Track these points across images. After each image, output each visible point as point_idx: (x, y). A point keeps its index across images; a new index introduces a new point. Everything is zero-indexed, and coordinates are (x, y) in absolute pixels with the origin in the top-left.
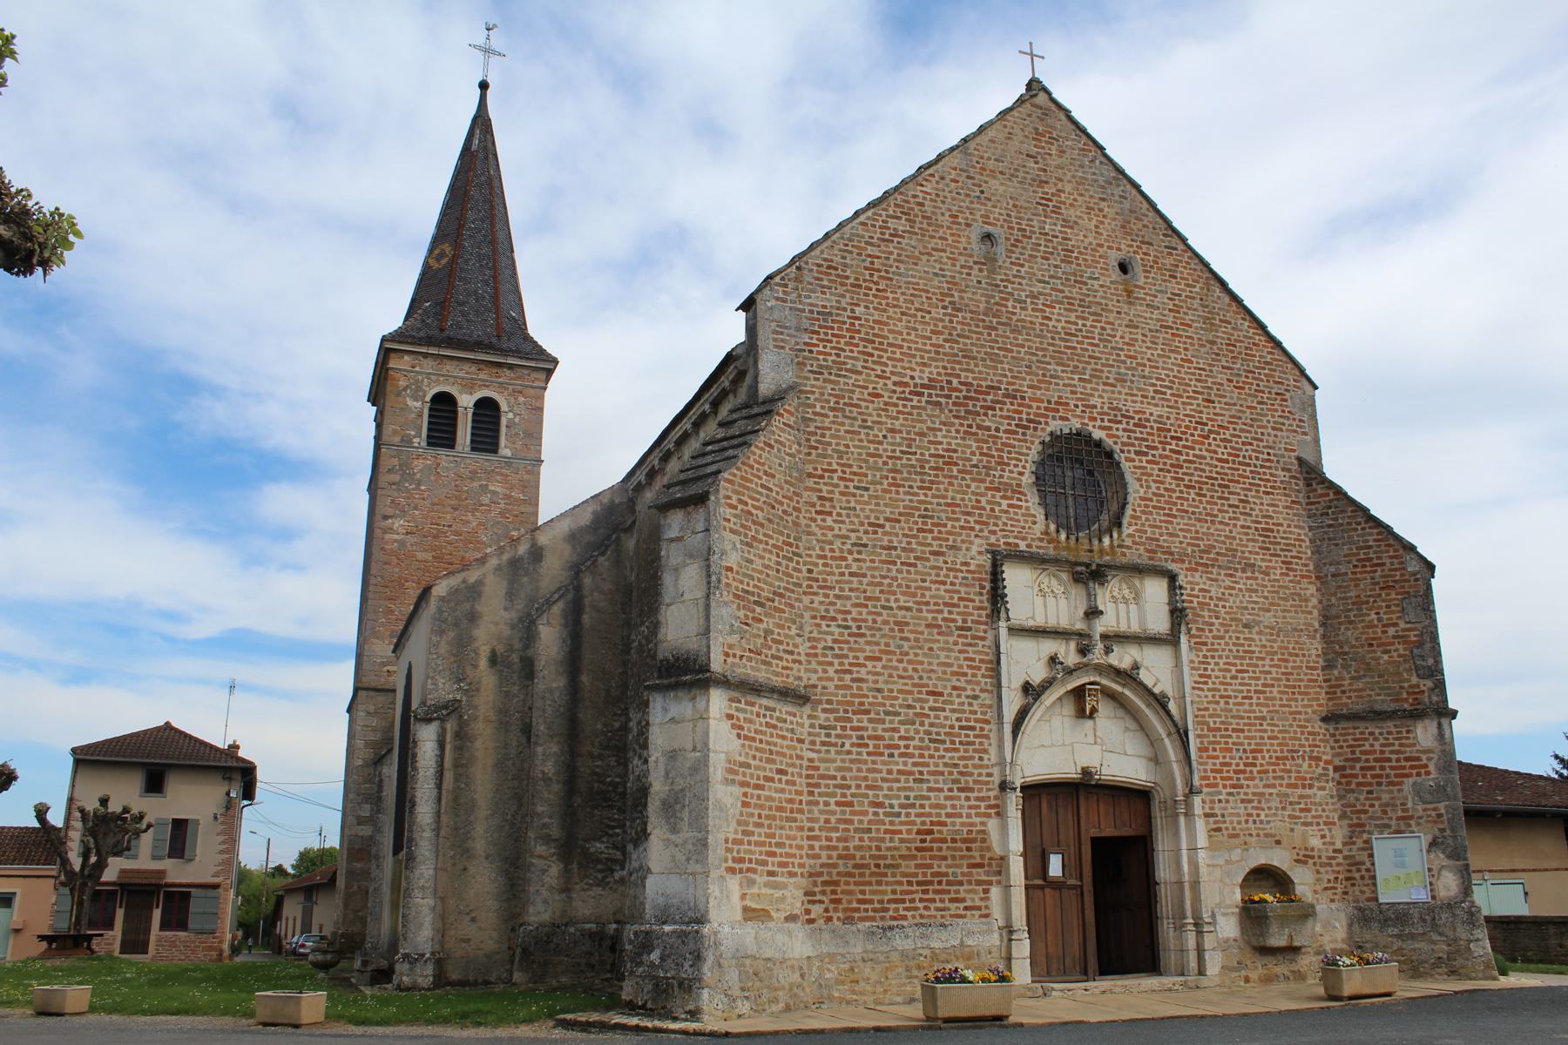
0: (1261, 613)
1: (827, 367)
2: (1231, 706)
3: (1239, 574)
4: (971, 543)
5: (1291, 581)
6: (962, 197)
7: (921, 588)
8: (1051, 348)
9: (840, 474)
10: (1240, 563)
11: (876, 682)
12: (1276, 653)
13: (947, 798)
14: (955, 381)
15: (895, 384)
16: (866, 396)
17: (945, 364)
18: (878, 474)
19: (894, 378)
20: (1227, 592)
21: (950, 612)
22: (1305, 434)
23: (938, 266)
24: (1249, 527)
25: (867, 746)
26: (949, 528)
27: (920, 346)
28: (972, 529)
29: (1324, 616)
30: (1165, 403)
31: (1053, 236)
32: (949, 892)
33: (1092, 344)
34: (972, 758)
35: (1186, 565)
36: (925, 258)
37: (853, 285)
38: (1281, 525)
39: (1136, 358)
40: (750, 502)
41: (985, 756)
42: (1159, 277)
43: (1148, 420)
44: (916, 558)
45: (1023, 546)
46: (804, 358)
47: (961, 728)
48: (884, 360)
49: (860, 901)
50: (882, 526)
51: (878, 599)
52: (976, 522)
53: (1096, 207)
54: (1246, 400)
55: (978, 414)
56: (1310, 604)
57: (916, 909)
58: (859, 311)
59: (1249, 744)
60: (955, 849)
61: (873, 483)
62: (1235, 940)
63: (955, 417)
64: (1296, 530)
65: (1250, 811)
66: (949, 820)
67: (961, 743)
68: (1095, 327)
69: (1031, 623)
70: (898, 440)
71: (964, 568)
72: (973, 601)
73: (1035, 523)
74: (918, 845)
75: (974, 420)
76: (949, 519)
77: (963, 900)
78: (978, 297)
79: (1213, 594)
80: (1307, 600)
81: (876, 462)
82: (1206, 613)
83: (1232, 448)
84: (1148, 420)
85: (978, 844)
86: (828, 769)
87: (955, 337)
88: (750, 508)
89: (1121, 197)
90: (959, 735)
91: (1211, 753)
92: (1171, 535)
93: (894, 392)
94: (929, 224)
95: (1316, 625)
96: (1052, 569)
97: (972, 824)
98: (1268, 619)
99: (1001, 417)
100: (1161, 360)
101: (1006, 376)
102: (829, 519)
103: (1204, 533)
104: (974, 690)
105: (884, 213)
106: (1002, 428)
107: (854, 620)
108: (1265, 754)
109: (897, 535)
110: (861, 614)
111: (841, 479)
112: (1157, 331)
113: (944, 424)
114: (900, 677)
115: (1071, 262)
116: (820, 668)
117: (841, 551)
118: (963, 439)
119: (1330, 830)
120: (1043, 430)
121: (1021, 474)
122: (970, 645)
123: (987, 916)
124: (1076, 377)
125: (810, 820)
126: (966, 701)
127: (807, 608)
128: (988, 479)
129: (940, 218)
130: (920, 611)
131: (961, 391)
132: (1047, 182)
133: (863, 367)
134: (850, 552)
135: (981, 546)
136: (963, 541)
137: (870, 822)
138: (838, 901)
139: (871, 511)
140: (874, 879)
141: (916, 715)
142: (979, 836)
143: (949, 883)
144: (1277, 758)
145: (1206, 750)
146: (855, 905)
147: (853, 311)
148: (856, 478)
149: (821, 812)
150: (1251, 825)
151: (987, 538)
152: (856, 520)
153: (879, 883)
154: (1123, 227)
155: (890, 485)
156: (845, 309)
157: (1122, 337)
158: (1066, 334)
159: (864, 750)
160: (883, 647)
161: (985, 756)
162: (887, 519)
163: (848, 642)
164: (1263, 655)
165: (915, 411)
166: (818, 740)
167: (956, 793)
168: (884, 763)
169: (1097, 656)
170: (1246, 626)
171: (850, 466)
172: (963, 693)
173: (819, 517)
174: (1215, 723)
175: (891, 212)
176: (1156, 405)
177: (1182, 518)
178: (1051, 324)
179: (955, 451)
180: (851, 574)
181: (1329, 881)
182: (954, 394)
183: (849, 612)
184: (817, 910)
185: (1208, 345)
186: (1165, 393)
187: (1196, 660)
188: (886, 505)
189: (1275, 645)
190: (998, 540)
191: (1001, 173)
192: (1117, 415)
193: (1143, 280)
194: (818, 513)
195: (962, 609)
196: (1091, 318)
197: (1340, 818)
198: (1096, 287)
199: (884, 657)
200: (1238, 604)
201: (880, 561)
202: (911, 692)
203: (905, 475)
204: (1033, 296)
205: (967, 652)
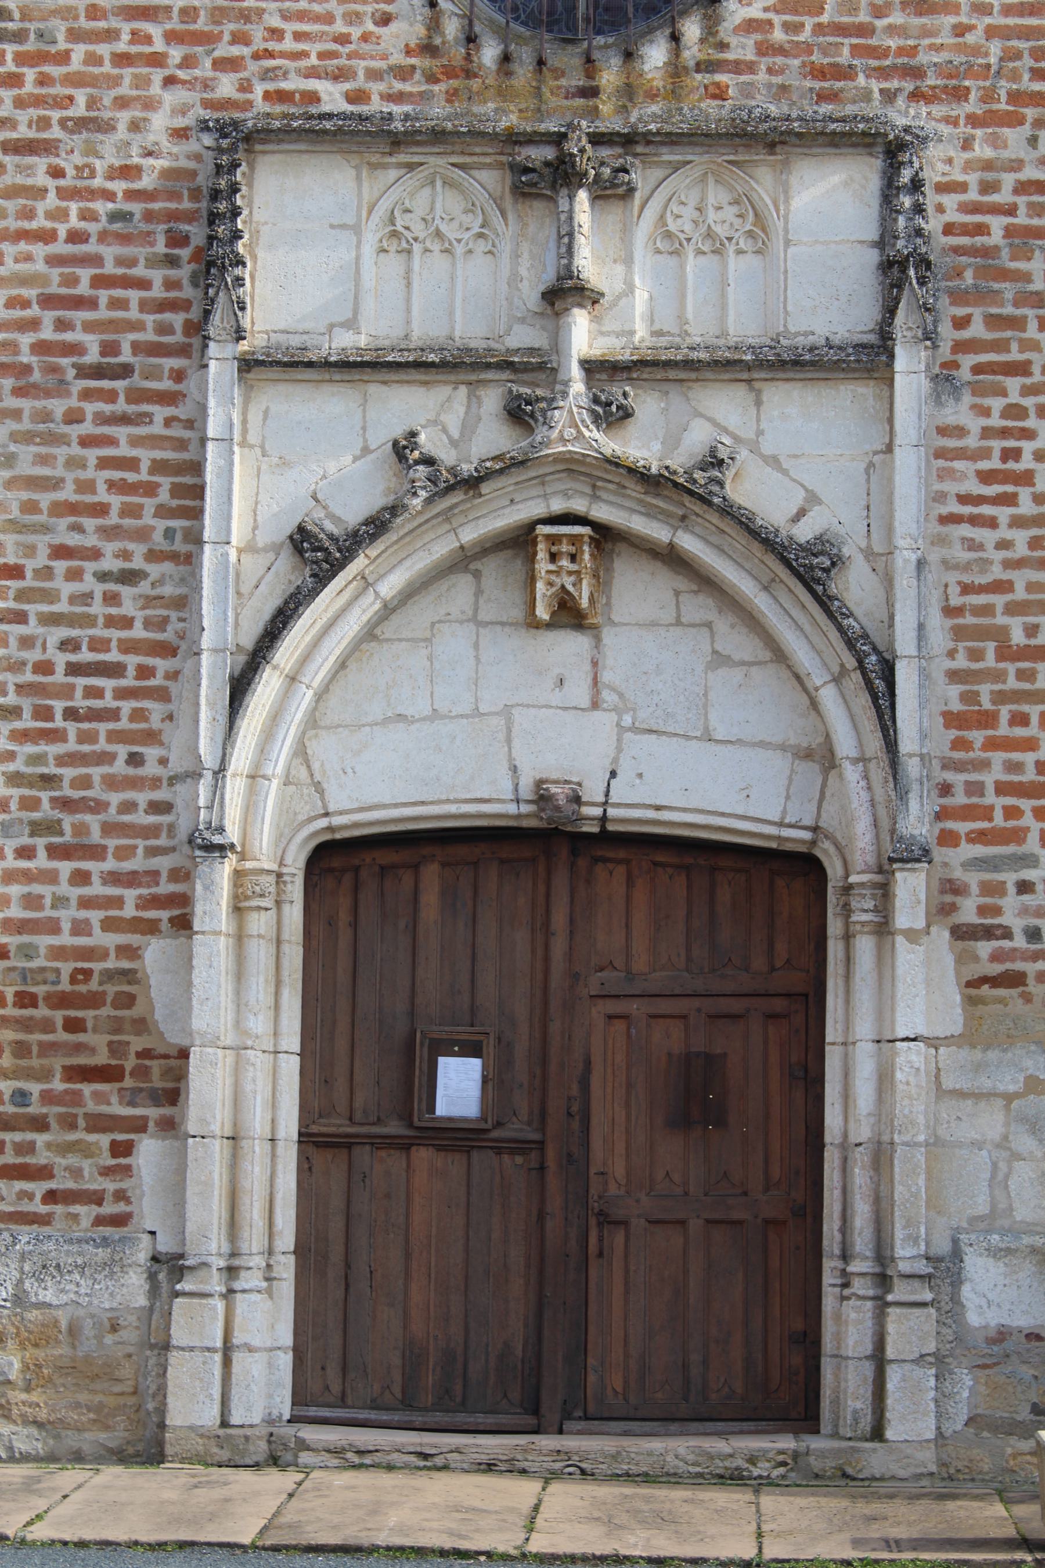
4: (150, 105)
21: (62, 325)
28: (157, 60)
35: (972, 106)
47: (74, 669)
52: (171, 37)
67: (71, 714)
71: (119, 186)
72: (143, 284)
73: (385, 20)
76: (75, 35)
77: (44, 1173)
85: (106, 1011)
90: (67, 691)
91: (1003, 729)
96: (437, 162)
104: (126, 555)
122: (124, 419)
123: (120, 1220)
126: (99, 589)
142: (111, 989)
145: (988, 719)
151: (206, 85)
161: (151, 753)
172: (90, 567)
187: (975, 424)
190: (245, 87)
195: (103, 313)
205: (112, 442)
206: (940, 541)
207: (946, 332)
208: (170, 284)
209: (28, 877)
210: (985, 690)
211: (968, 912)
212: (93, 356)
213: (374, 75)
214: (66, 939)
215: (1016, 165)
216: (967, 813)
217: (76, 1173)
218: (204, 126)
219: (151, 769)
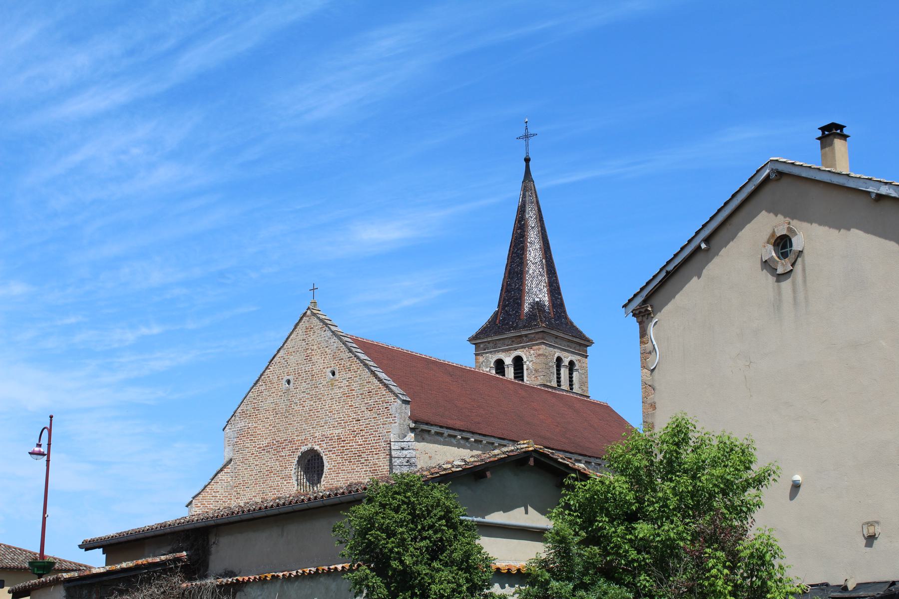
9: (242, 484)
16: (250, 455)
19: (258, 446)
22: (395, 423)
23: (272, 399)
24: (367, 471)
33: (318, 412)
38: (380, 466)
39: (332, 412)
40: (206, 503)
43: (334, 436)
55: (280, 452)
76: (269, 492)
83: (365, 438)
84: (334, 436)
88: (206, 505)
92: (338, 481)
93: (258, 451)
99: (287, 451)
101: (289, 434)
102: (239, 500)
111: (243, 486)
113: (270, 458)
118: (275, 462)
120: (299, 451)
121: (291, 470)
132: (308, 349)
133: (250, 445)
158: (310, 410)
176: (337, 429)
177: (342, 473)
179: (273, 467)
185: (360, 396)
186: (341, 423)
196: (318, 401)
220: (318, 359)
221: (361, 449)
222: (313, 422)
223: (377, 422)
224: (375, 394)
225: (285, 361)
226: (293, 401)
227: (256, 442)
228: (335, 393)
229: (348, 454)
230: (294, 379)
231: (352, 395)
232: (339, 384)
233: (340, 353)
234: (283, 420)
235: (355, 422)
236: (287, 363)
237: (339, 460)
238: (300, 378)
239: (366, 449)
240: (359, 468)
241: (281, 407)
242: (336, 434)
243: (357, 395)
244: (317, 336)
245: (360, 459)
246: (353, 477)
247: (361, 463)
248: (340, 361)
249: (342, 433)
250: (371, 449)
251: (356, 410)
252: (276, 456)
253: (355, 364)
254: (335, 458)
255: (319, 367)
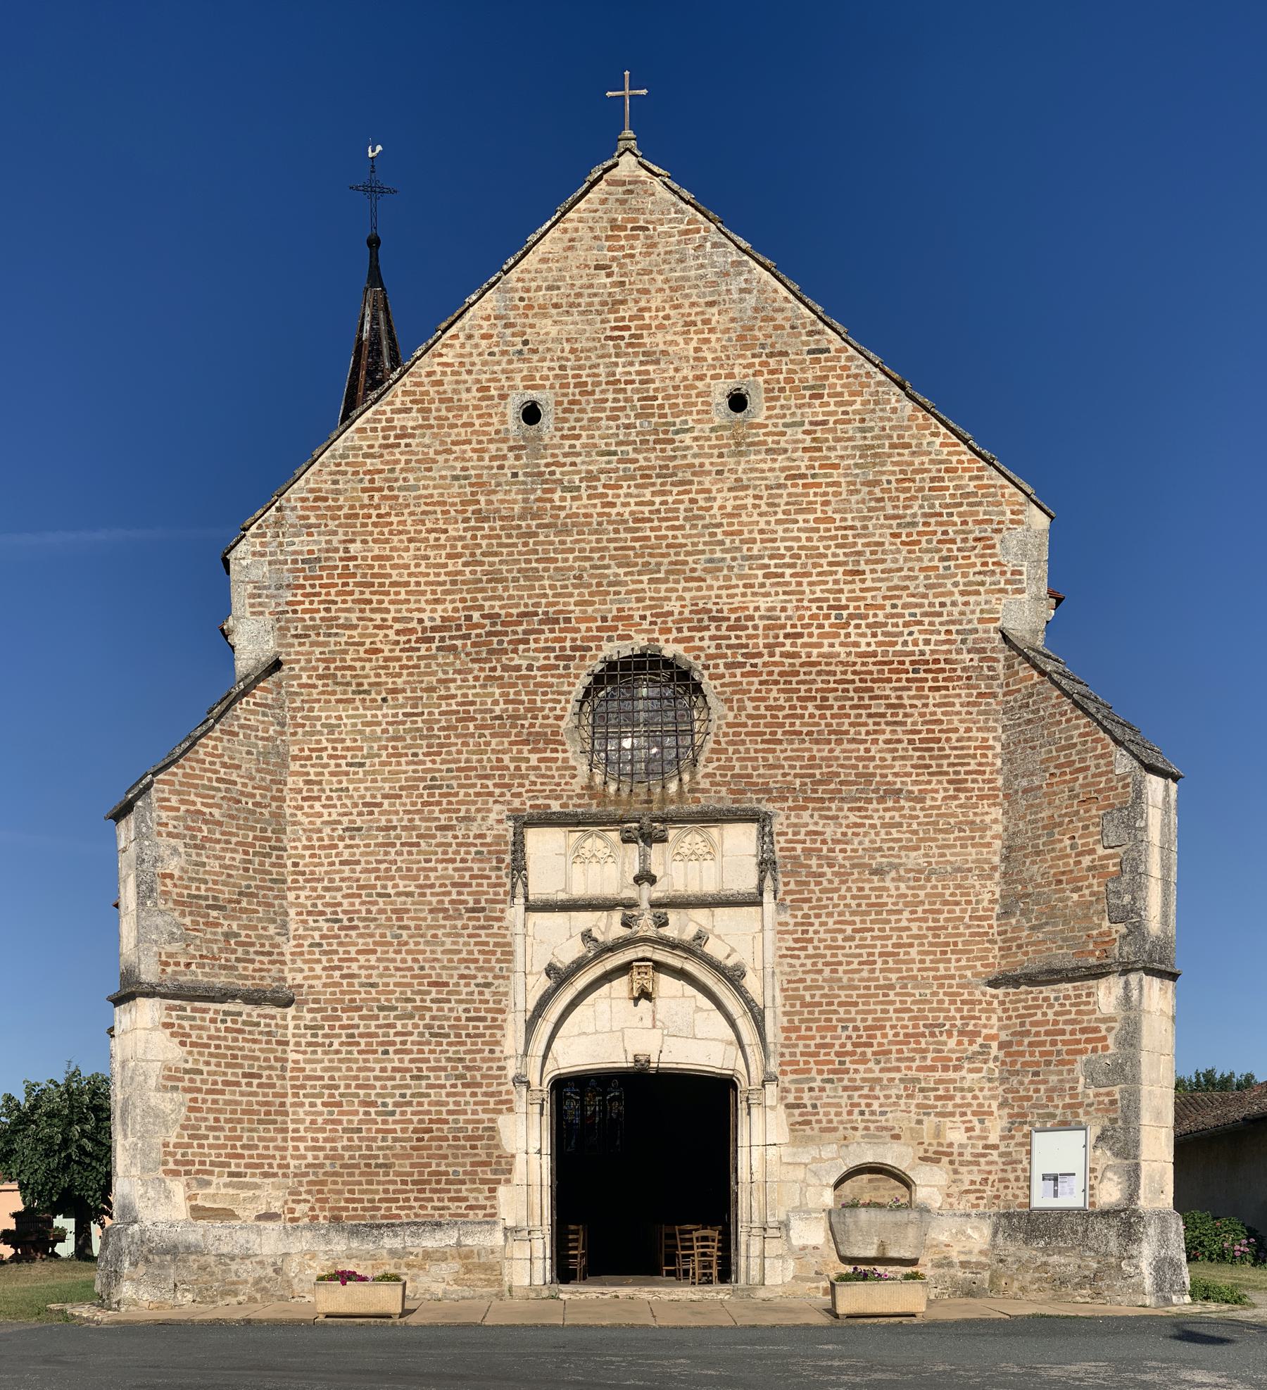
0: (903, 853)
1: (314, 628)
2: (840, 974)
3: (875, 805)
4: (489, 810)
5: (960, 806)
6: (497, 358)
7: (424, 869)
8: (612, 545)
9: (330, 751)
10: (876, 791)
11: (370, 976)
12: (922, 903)
13: (448, 1095)
14: (476, 616)
15: (398, 633)
16: (362, 655)
17: (465, 595)
18: (375, 745)
19: (397, 626)
20: (850, 832)
21: (459, 893)
22: (1021, 591)
23: (459, 465)
24: (899, 741)
25: (358, 1044)
26: (461, 797)
27: (432, 578)
28: (491, 794)
29: (1009, 847)
30: (780, 590)
31: (627, 382)
32: (449, 1191)
33: (673, 528)
34: (482, 1051)
36: (441, 458)
37: (347, 516)
38: (956, 730)
41: (497, 1049)
42: (793, 402)
43: (751, 618)
44: (418, 836)
45: (555, 806)
46: (288, 621)
47: (468, 1019)
48: (385, 605)
49: (347, 1201)
50: (380, 805)
51: (374, 887)
52: (495, 785)
53: (699, 319)
54: (920, 559)
55: (505, 652)
56: (989, 833)
57: (411, 1208)
58: (355, 548)
59: (864, 1020)
60: (457, 1147)
61: (370, 756)
62: (815, 1248)
63: (473, 661)
64: (980, 735)
65: (856, 1100)
66: (451, 1118)
67: (468, 1035)
68: (682, 502)
69: (562, 896)
70: (401, 701)
71: (478, 841)
72: (489, 877)
73: (574, 777)
74: (414, 1143)
75: (498, 661)
76: (461, 786)
77: (465, 1199)
78: (513, 496)
79: (828, 836)
80: (984, 828)
81: (373, 732)
82: (814, 862)
83: (885, 634)
84: (751, 618)
86: (314, 1070)
87: (479, 558)
89: (742, 291)
90: (466, 1027)
91: (803, 1033)
93: (397, 643)
94: (449, 409)
95: (996, 860)
97: (478, 1122)
98: (914, 859)
99: (535, 650)
100: (780, 528)
101: (545, 596)
102: (317, 805)
103: (822, 759)
105: (388, 408)
106: (536, 664)
107: (345, 912)
108: (888, 1030)
109: (397, 813)
110: (353, 904)
111: (330, 757)
112: (779, 486)
113: (459, 672)
114: (397, 969)
115: (653, 415)
116: (306, 967)
117: (331, 838)
119: (982, 1122)
120: (594, 657)
122: (483, 927)
124: (645, 578)
125: (293, 1121)
127: (292, 904)
128: (514, 731)
129: (464, 396)
130: (424, 895)
131: (483, 626)
133: (359, 619)
134: (342, 838)
135: (500, 813)
136: (478, 811)
137: (360, 1122)
138: (326, 1200)
139: (367, 789)
140: (363, 1179)
141: (416, 1008)
143: (448, 1182)
144: (906, 1035)
145: (798, 1029)
146: (343, 1204)
147: (346, 550)
148: (349, 754)
149: (307, 1113)
150: (856, 1116)
151: (509, 803)
152: (348, 802)
153: (370, 1183)
154: (741, 338)
155: (389, 756)
156: (336, 550)
157: (722, 507)
158: (636, 520)
159: (355, 1049)
160: (378, 939)
161: (497, 1049)
162: (385, 796)
163: (338, 937)
164: (900, 906)
165: (422, 663)
166: (303, 1041)
167: (460, 1089)
168: (377, 1061)
169: (646, 926)
170: (875, 872)
171: (343, 741)
173: (306, 804)
174: (813, 996)
175: (398, 405)
176: (767, 595)
177: (791, 742)
178: (614, 511)
179: (473, 703)
180: (342, 863)
181: (973, 1182)
182: (474, 632)
183: (340, 904)
184: (301, 1209)
185: (866, 489)
186: (782, 575)
187: (792, 921)
188: (384, 780)
189: (922, 893)
190: (523, 803)
191: (556, 306)
192: (703, 618)
193: (765, 413)
194: (304, 799)
195: (474, 889)
196: (675, 490)
197: (1001, 1106)
198: (688, 442)
199: (379, 949)
200: (867, 844)
201: (377, 845)
202: (410, 985)
203: (409, 741)
204: (591, 477)
206: (780, 964)
207: (781, 888)
208: (498, 877)
209: (455, 1094)
210: (796, 1018)
211: (791, 1099)
212: (471, 905)
213: (570, 797)
214: (469, 1116)
215: (806, 825)
216: (790, 1063)
217: (476, 1199)
218: (509, 818)
219: (497, 1055)
220: (672, 343)
221: (871, 667)
222: (653, 561)
223: (941, 585)
224: (930, 489)
225: (513, 335)
226: (560, 481)
227: (387, 611)
228: (752, 470)
229: (813, 682)
230: (559, 403)
231: (828, 485)
232: (770, 439)
233: (770, 330)
234: (514, 545)
235: (840, 576)
236: (526, 343)
237: (776, 699)
238: (588, 403)
239: (890, 671)
240: (863, 730)
241: (500, 496)
242: (757, 609)
243: (849, 483)
244: (664, 261)
245: (867, 702)
246: (837, 758)
247: (869, 715)
248: (771, 361)
249: (784, 609)
250: (915, 671)
251: (845, 537)
252: (487, 666)
253: (839, 377)
254: (758, 691)
255: (677, 370)
